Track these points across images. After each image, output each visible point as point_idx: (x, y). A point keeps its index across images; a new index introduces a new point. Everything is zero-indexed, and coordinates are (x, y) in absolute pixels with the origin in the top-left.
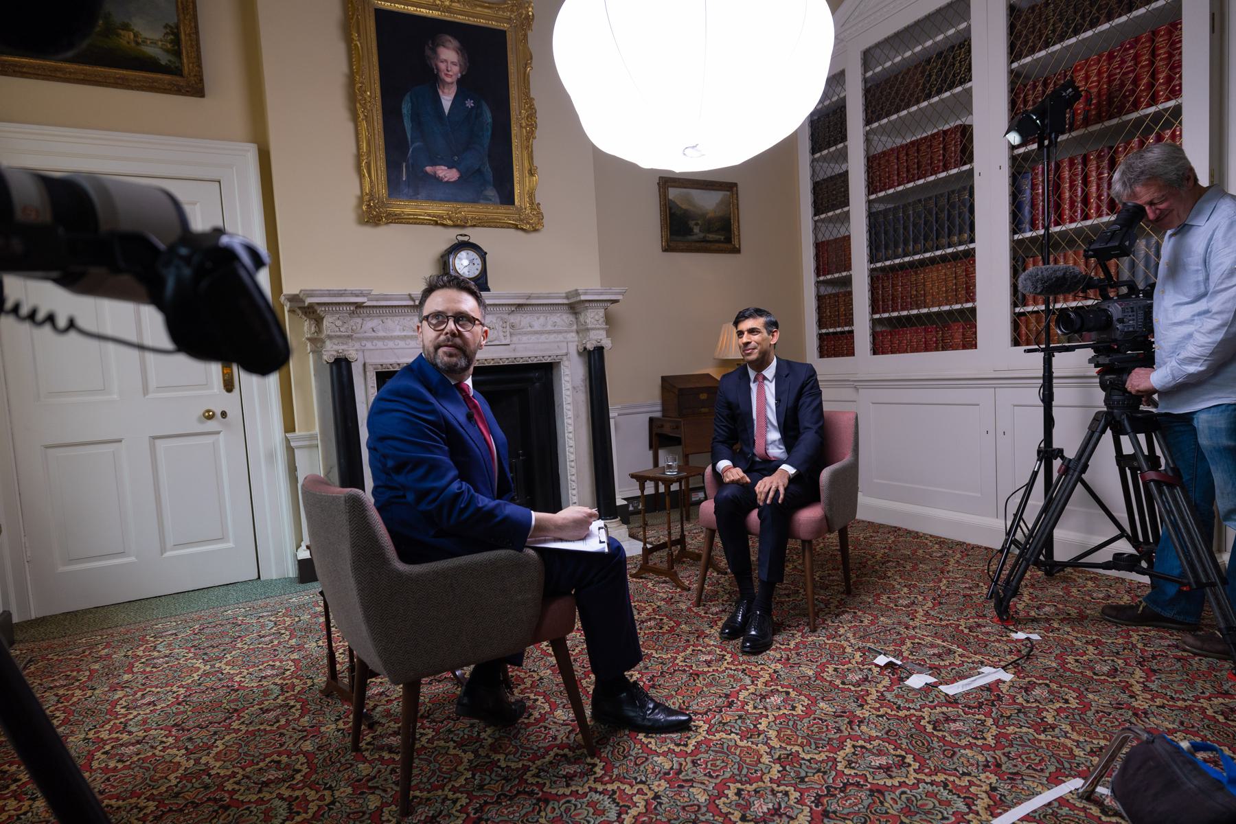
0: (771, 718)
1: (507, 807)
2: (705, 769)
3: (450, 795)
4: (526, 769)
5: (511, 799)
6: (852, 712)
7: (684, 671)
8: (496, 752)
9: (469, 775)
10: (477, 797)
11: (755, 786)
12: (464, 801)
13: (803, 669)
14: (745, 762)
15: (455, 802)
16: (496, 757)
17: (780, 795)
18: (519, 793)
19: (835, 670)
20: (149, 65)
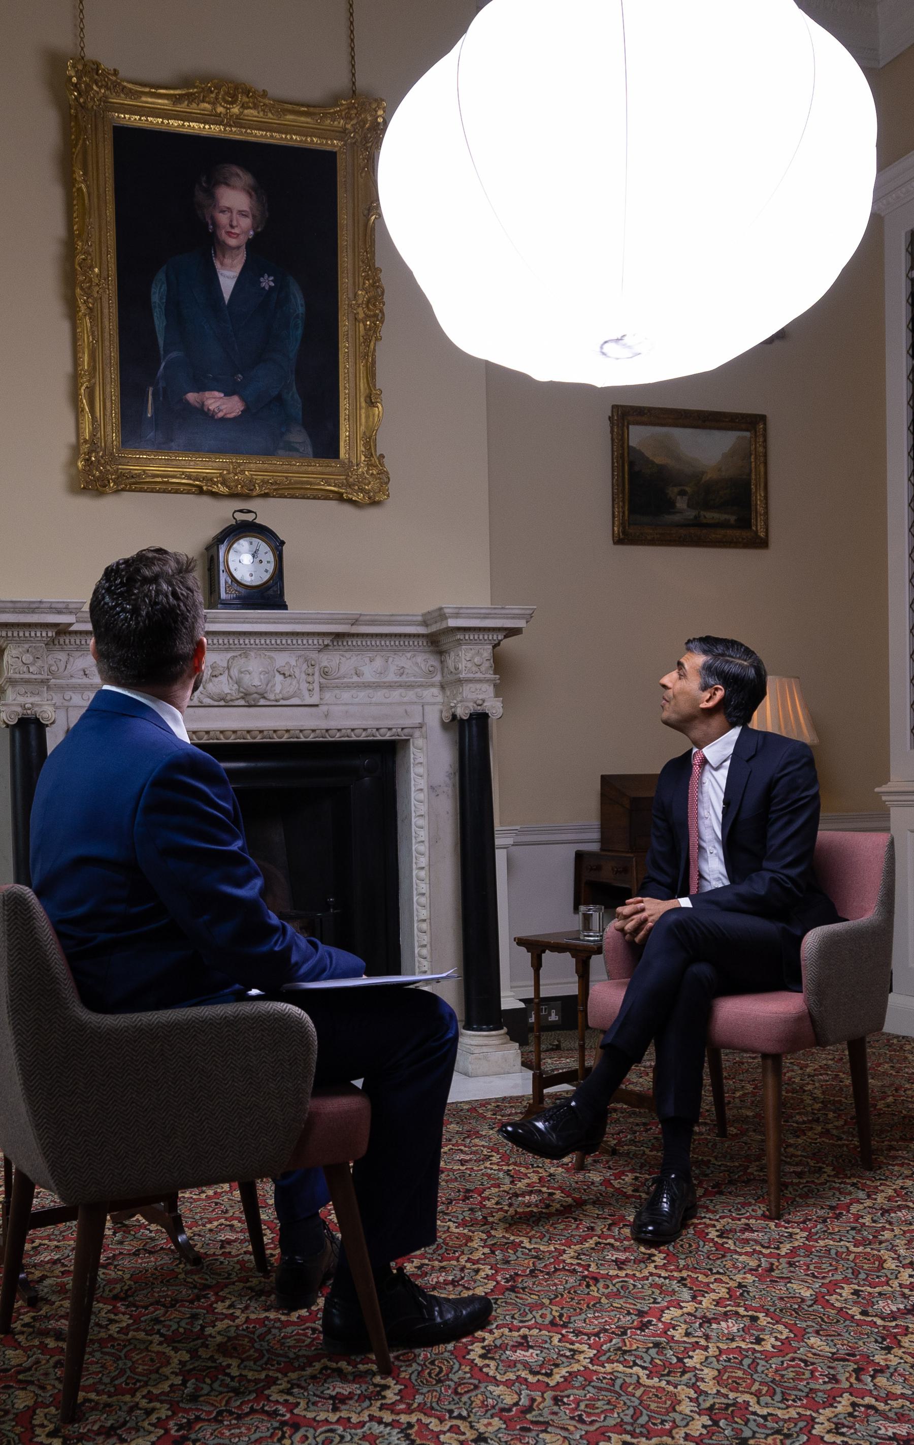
0: (713, 1351)
1: (229, 1427)
3: (144, 1403)
5: (239, 1417)
6: (867, 1357)
7: (574, 1272)
9: (178, 1380)
10: (186, 1411)
12: (164, 1413)
13: (794, 1286)
15: (149, 1413)
18: (253, 1411)
19: (856, 1293)
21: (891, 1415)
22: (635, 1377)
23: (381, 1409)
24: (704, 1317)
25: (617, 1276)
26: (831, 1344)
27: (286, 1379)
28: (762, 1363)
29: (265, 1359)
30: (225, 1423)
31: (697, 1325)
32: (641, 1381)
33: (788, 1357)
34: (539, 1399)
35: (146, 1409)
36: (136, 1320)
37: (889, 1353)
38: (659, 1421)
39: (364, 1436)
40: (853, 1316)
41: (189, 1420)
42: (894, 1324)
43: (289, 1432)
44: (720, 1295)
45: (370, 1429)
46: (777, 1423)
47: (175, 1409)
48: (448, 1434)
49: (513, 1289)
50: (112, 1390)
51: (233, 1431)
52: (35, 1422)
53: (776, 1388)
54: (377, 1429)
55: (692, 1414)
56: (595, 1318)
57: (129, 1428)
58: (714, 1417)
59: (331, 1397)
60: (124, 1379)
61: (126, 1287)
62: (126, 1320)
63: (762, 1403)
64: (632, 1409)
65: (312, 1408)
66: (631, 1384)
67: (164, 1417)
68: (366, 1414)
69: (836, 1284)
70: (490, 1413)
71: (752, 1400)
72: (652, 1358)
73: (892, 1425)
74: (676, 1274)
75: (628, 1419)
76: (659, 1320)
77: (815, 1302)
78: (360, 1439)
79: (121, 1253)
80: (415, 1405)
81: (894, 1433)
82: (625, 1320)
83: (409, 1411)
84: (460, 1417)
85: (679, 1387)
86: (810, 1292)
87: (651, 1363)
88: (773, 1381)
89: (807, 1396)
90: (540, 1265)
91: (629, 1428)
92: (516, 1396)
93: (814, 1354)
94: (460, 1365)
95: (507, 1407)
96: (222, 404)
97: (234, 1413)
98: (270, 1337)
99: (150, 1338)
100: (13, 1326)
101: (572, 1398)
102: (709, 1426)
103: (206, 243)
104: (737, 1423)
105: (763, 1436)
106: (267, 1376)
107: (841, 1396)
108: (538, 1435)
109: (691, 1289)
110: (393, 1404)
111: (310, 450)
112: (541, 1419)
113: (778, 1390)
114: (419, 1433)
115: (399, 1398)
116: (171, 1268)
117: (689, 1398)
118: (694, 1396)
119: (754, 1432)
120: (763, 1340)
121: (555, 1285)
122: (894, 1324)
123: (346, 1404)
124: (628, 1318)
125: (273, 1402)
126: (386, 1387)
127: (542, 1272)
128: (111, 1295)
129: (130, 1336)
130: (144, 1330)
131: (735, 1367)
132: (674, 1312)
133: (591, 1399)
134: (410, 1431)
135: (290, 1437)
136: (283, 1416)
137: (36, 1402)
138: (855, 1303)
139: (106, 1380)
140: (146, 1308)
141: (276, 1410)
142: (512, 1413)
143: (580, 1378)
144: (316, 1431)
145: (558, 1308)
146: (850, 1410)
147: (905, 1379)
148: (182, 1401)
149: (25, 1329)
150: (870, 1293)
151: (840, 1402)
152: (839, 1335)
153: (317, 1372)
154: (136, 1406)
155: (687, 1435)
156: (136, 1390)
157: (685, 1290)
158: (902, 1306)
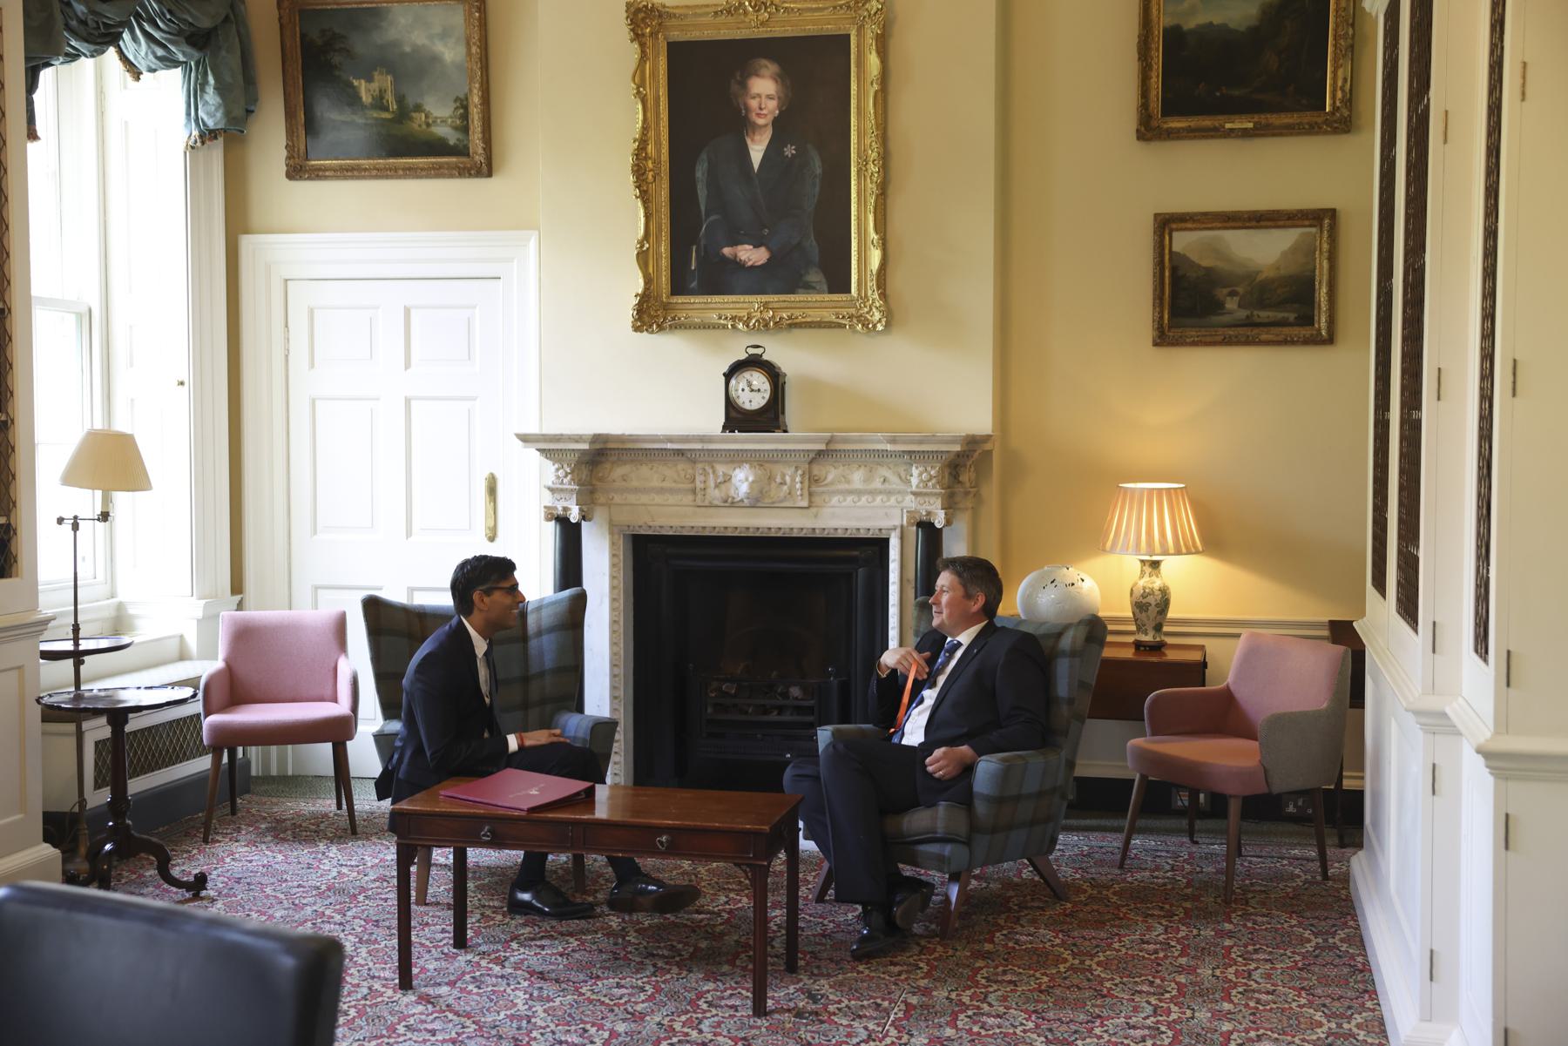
20: (436, 147)
96: (753, 255)
103: (740, 124)
111: (825, 287)
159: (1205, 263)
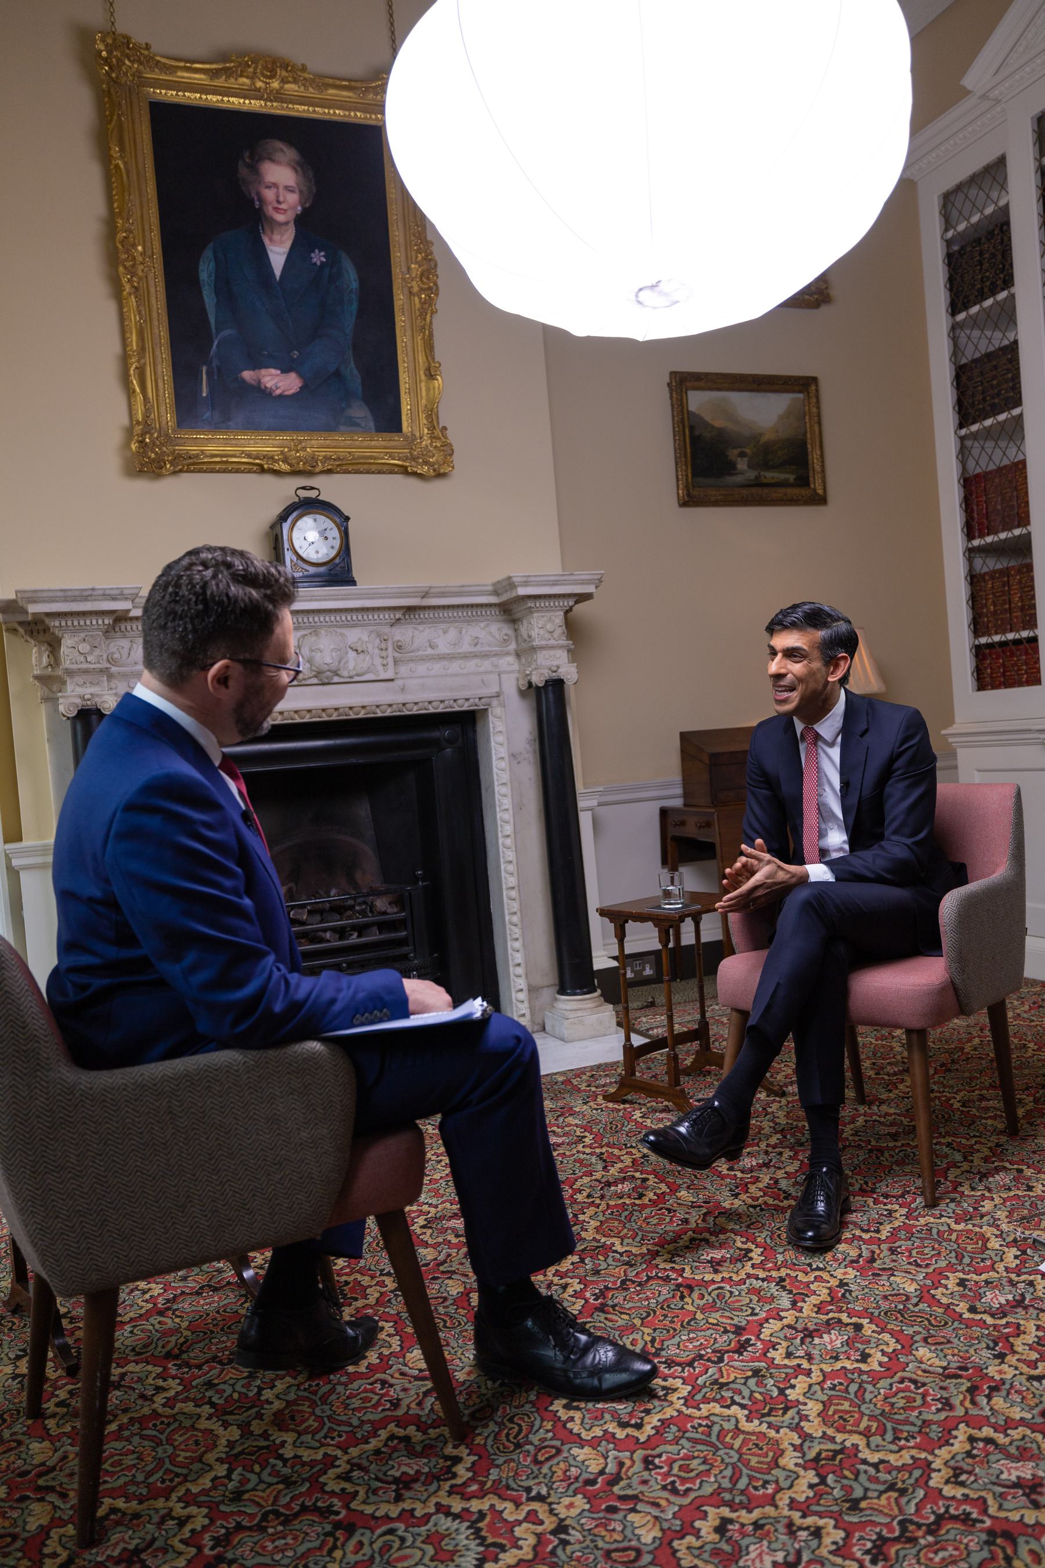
0: (817, 1376)
2: (668, 1474)
3: (179, 1510)
4: (329, 1462)
5: (286, 1521)
6: (979, 1369)
7: (667, 1279)
8: (282, 1428)
9: (221, 1470)
10: (225, 1516)
11: (756, 1514)
14: (747, 1464)
15: (182, 1522)
16: (278, 1437)
17: (803, 1535)
19: (962, 1283)
21: (1013, 1450)
22: (733, 1421)
23: (450, 1493)
24: (806, 1329)
25: (713, 1282)
26: (941, 1355)
27: (346, 1458)
28: (869, 1388)
29: (325, 1430)
30: (271, 1531)
31: (798, 1341)
32: (740, 1425)
33: (896, 1378)
34: (628, 1463)
35: (179, 1519)
36: (186, 1385)
37: (1003, 1362)
38: (760, 1483)
39: (428, 1536)
40: (961, 1315)
41: (227, 1529)
42: (1004, 1321)
43: (342, 1539)
44: (821, 1298)
45: (436, 1525)
46: (889, 1473)
47: (214, 1514)
48: (525, 1525)
49: (602, 1309)
50: (144, 1491)
51: (277, 1543)
52: (47, 1551)
53: (888, 1425)
54: (445, 1524)
55: (796, 1469)
56: (690, 1340)
57: (156, 1550)
58: (821, 1471)
59: (396, 1481)
60: (160, 1473)
61: (182, 1340)
62: (174, 1386)
63: (873, 1446)
64: (730, 1468)
65: (373, 1498)
66: (729, 1431)
67: (199, 1528)
68: (434, 1500)
69: (940, 1273)
70: (573, 1487)
71: (861, 1442)
72: (752, 1392)
73: (1014, 1465)
74: (774, 1274)
75: (726, 1484)
76: (758, 1338)
77: (921, 1299)
78: (423, 1542)
79: (183, 1293)
80: (489, 1484)
81: (1018, 1477)
82: (722, 1341)
83: (481, 1495)
84: (540, 1498)
85: (782, 1431)
86: (915, 1286)
87: (750, 1399)
88: (883, 1413)
89: (920, 1432)
90: (631, 1274)
91: (727, 1496)
92: (602, 1461)
93: (924, 1371)
94: (542, 1420)
95: (592, 1477)
97: (283, 1514)
98: (333, 1397)
99: (198, 1410)
100: (45, 1406)
101: (664, 1458)
102: (817, 1485)
104: (846, 1477)
105: (876, 1494)
106: (325, 1455)
107: (956, 1428)
108: (625, 1517)
109: (790, 1292)
110: (465, 1484)
112: (629, 1492)
113: (889, 1425)
114: (492, 1524)
115: (470, 1474)
116: (235, 1308)
117: (793, 1445)
118: (798, 1442)
119: (866, 1490)
120: (869, 1355)
121: (648, 1299)
122: (1004, 1321)
123: (410, 1489)
124: (725, 1338)
125: (327, 1493)
126: (457, 1460)
127: (633, 1282)
128: (164, 1351)
129: (176, 1410)
130: (193, 1400)
131: (843, 1392)
132: (774, 1325)
133: (686, 1458)
134: (480, 1525)
135: (343, 1545)
136: (338, 1513)
137: (52, 1519)
138: (962, 1296)
139: (140, 1477)
140: (199, 1367)
141: (331, 1506)
142: (598, 1486)
143: (674, 1428)
144: (373, 1533)
145: (650, 1331)
146: (968, 1447)
147: (1023, 1398)
148: (223, 1502)
149: (58, 1410)
150: (976, 1282)
151: (956, 1437)
152: (949, 1342)
153: (380, 1445)
154: (169, 1515)
155: (792, 1500)
156: (172, 1489)
157: (784, 1294)
158: (1010, 1297)
159: (718, 423)
